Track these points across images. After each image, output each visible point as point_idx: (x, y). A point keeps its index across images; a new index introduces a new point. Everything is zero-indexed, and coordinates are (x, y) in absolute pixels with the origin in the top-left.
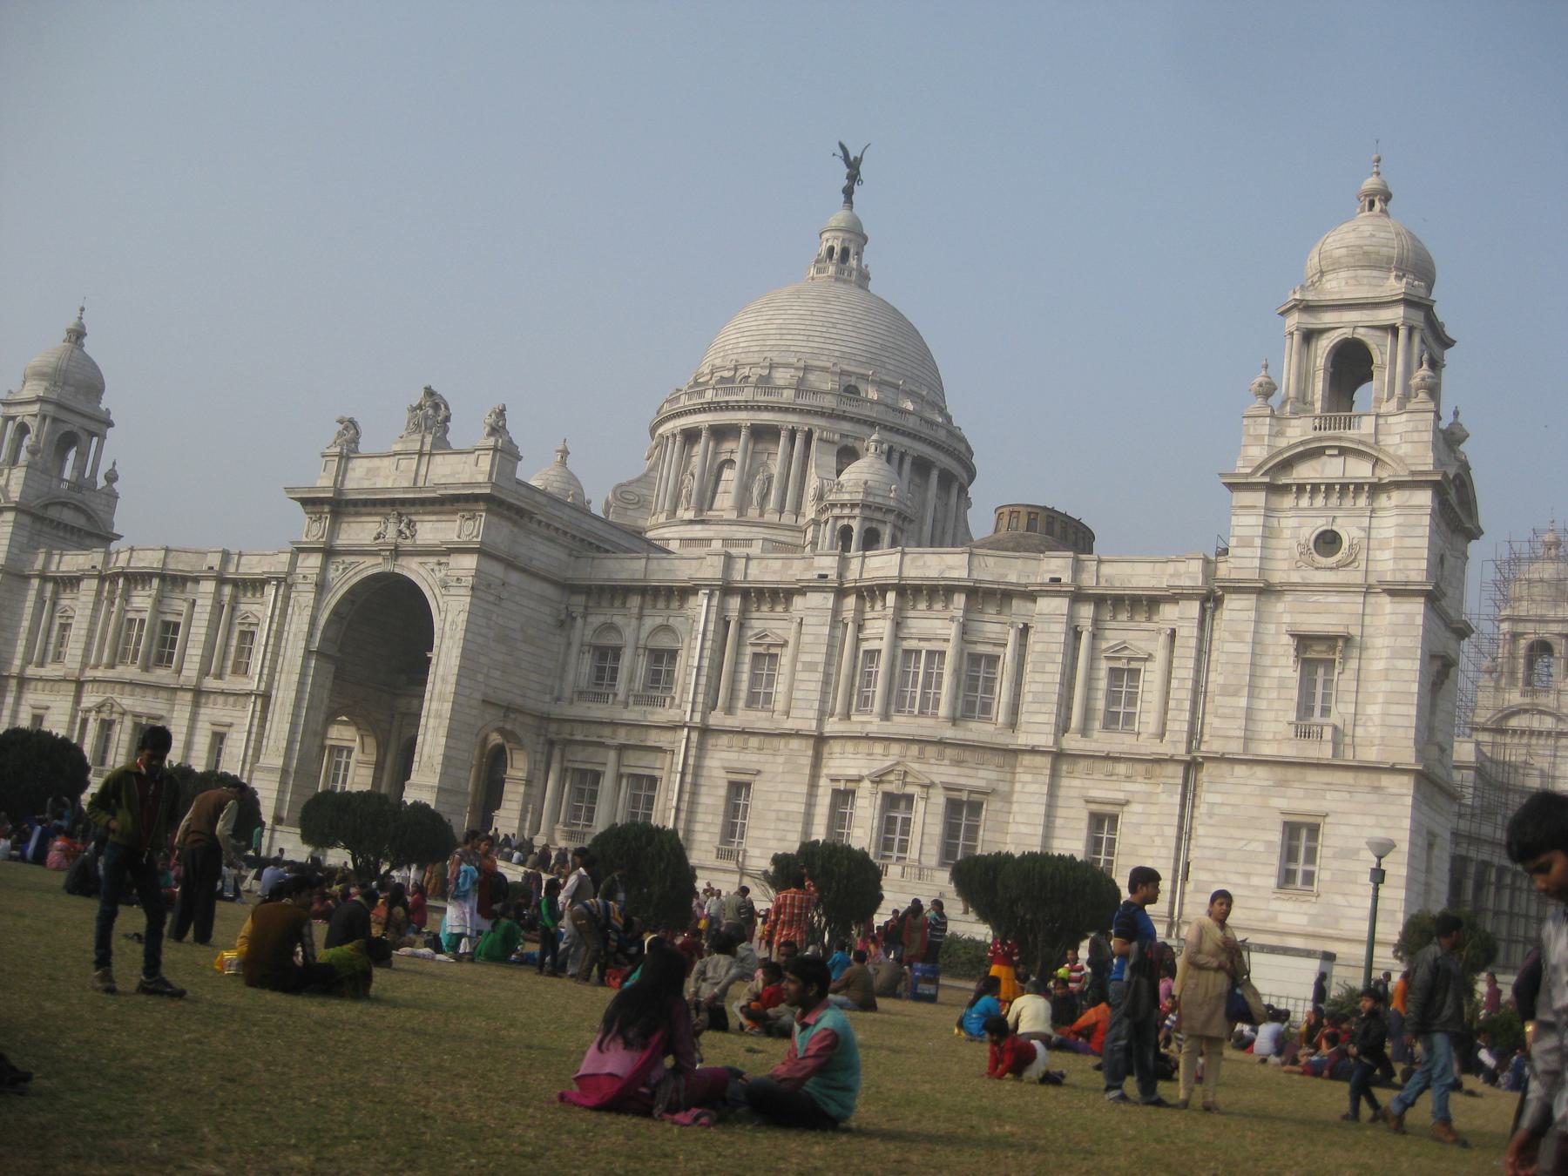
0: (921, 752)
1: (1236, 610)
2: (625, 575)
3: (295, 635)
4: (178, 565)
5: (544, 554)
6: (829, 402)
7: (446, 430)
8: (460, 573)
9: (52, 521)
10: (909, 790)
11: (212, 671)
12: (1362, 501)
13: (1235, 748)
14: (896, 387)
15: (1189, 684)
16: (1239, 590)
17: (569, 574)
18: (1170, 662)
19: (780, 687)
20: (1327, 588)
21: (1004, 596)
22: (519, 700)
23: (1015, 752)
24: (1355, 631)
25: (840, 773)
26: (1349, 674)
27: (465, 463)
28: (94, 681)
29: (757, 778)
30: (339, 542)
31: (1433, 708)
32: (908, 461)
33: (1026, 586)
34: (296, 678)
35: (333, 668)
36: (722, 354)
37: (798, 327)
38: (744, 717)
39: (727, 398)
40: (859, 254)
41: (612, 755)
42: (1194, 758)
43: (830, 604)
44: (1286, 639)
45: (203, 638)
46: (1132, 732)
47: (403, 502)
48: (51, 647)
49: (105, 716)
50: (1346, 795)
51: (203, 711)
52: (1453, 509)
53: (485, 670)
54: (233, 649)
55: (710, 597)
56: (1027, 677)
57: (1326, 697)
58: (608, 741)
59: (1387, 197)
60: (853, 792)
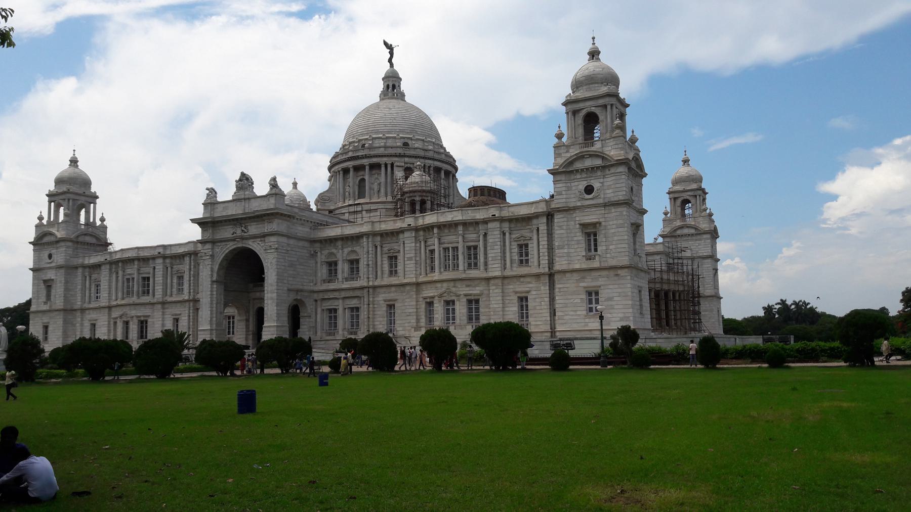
1: (558, 219)
3: (205, 276)
5: (302, 230)
6: (399, 151)
7: (253, 188)
8: (270, 244)
9: (81, 242)
11: (168, 294)
12: (599, 173)
13: (565, 267)
14: (423, 140)
15: (546, 246)
16: (559, 210)
17: (312, 236)
18: (538, 240)
19: (400, 268)
20: (589, 206)
21: (476, 223)
22: (301, 287)
23: (488, 279)
24: (601, 220)
26: (602, 236)
28: (117, 306)
30: (218, 238)
31: (635, 243)
32: (432, 169)
33: (483, 219)
35: (223, 287)
36: (352, 136)
38: (387, 280)
39: (357, 154)
40: (399, 86)
41: (341, 301)
42: (551, 273)
44: (578, 226)
45: (161, 281)
46: (528, 266)
47: (242, 219)
48: (92, 295)
50: (606, 279)
52: (635, 170)
53: (287, 279)
54: (175, 284)
55: (368, 238)
56: (489, 252)
57: (596, 245)
58: (338, 297)
60: (432, 303)
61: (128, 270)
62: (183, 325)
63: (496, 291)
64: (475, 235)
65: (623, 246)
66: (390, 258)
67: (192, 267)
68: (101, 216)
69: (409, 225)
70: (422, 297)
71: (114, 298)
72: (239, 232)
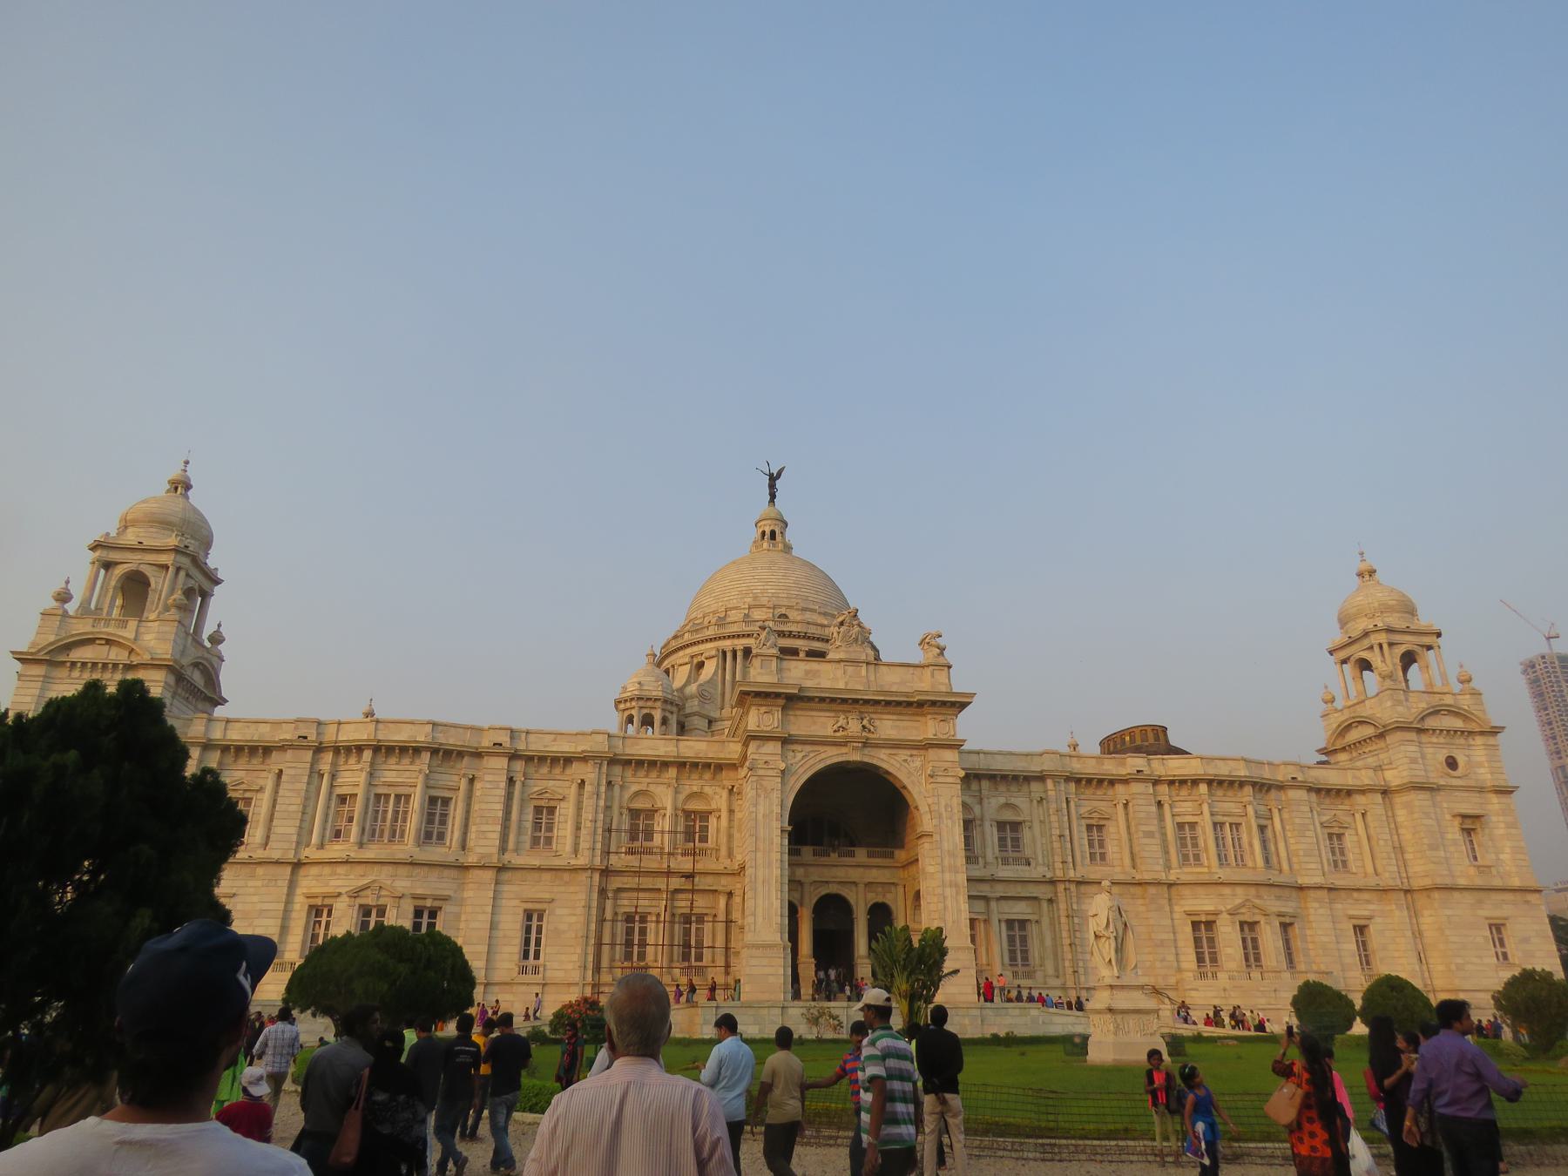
4: (450, 740)
10: (1256, 918)
11: (511, 845)
12: (1462, 741)
13: (1448, 881)
23: (1301, 888)
25: (1199, 909)
27: (913, 674)
36: (751, 595)
43: (1151, 791)
44: (1448, 817)
45: (500, 814)
46: (1348, 872)
47: (867, 702)
49: (369, 899)
51: (506, 888)
58: (989, 895)
59: (1372, 572)
63: (1321, 911)
64: (1262, 808)
65: (1522, 857)
66: (1089, 827)
67: (603, 789)
68: (216, 628)
69: (1138, 771)
70: (1185, 911)
72: (854, 727)
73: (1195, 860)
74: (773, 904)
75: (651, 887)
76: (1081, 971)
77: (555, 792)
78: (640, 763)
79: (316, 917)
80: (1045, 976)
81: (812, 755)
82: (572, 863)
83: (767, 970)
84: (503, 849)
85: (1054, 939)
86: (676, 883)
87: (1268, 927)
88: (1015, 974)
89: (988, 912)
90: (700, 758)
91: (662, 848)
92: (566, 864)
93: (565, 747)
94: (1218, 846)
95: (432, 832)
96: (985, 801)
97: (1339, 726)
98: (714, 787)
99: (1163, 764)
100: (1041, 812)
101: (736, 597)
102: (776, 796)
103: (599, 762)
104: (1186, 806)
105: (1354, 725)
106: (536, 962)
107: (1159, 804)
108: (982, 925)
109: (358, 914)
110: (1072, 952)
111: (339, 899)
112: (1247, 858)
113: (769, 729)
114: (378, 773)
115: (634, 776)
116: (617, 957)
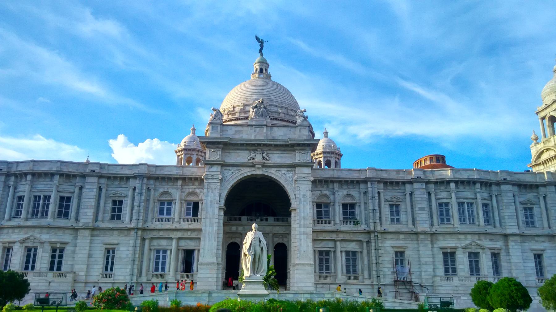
0: (479, 237)
2: (327, 176)
4: (71, 170)
8: (304, 175)
11: (100, 218)
23: (506, 236)
29: (406, 249)
34: (217, 220)
37: (274, 93)
40: (266, 70)
43: (424, 187)
45: (93, 204)
46: (535, 227)
49: (30, 245)
58: (336, 239)
61: (39, 186)
62: (120, 257)
63: (516, 247)
66: (391, 206)
67: (144, 191)
69: (417, 177)
70: (439, 247)
71: (7, 217)
72: (258, 157)
73: (447, 222)
74: (213, 243)
75: (167, 237)
76: (381, 276)
77: (122, 193)
78: (163, 178)
79: (7, 252)
80: (363, 279)
81: (237, 172)
82: (128, 226)
83: (208, 275)
84: (96, 220)
85: (369, 261)
86: (179, 234)
87: (484, 255)
88: (348, 278)
89: (335, 247)
90: (192, 175)
91: (174, 219)
92: (125, 226)
93: (127, 172)
94: (460, 214)
95: (63, 211)
96: (337, 193)
97: (538, 152)
98: (200, 189)
99: (432, 174)
100: (366, 199)
101: (238, 101)
102: (217, 193)
103: (142, 178)
104: (443, 196)
105: (545, 151)
106: (111, 273)
107: (429, 194)
108: (332, 253)
109: (25, 251)
110: (377, 267)
111: (16, 244)
112: (476, 220)
113: (214, 159)
114: (34, 186)
115: (160, 184)
116: (151, 270)
